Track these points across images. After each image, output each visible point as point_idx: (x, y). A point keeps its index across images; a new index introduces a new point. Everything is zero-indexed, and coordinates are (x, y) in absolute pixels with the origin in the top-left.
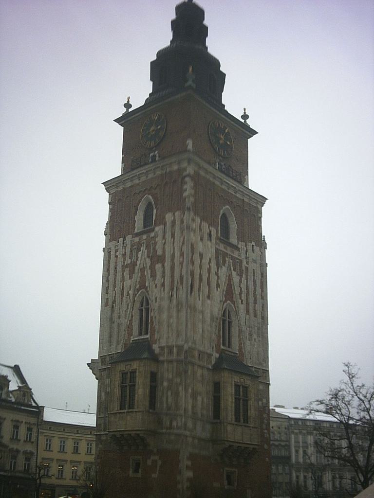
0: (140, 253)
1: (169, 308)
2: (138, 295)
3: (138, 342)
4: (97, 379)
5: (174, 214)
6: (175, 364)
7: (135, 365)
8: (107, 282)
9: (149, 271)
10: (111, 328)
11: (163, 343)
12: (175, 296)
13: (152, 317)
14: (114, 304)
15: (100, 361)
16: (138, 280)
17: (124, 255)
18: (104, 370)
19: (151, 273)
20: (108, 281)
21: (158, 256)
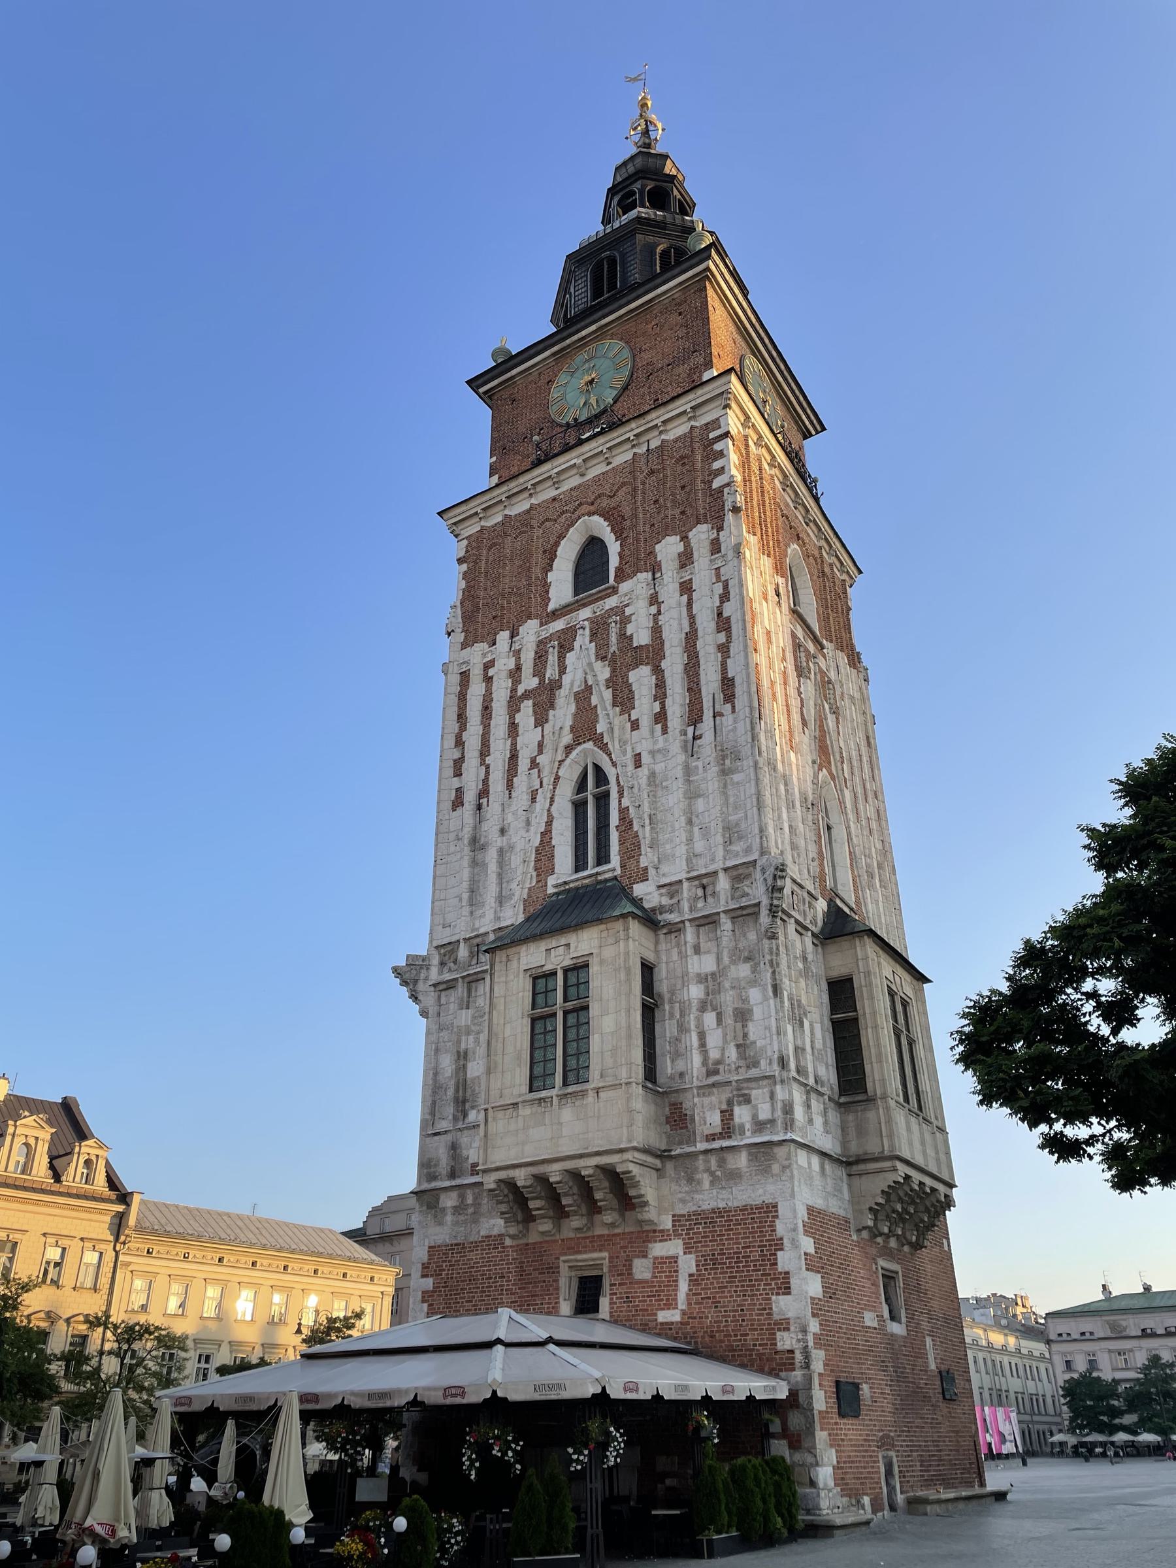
0: (570, 658)
1: (688, 771)
2: (568, 761)
3: (577, 889)
4: (424, 1013)
5: (685, 538)
6: (726, 924)
7: (584, 942)
8: (456, 746)
9: (608, 695)
10: (474, 863)
11: (676, 871)
12: (708, 736)
13: (623, 812)
14: (484, 801)
15: (435, 961)
16: (569, 722)
17: (515, 674)
18: (450, 985)
19: (615, 696)
20: (459, 743)
21: (640, 647)
